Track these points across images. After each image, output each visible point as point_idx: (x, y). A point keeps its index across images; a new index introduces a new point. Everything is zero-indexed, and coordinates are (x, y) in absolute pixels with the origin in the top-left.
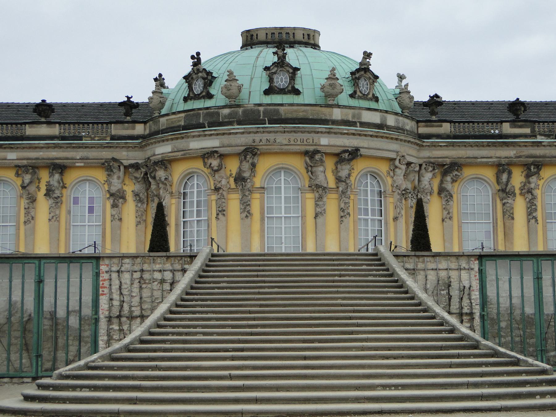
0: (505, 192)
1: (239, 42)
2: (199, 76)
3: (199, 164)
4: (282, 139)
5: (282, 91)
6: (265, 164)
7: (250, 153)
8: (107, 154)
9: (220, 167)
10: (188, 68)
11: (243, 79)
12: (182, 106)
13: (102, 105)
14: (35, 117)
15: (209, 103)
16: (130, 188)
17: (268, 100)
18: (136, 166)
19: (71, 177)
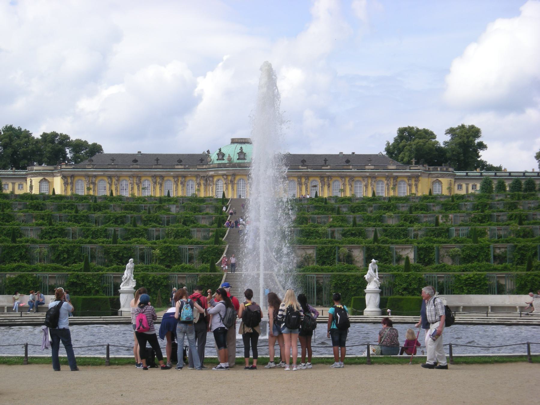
0: (300, 184)
1: (230, 141)
2: (221, 155)
3: (221, 177)
4: (241, 172)
5: (241, 159)
6: (237, 178)
7: (234, 175)
8: (196, 173)
9: (227, 178)
10: (218, 151)
11: (232, 156)
12: (216, 162)
13: (188, 155)
14: (177, 163)
15: (223, 162)
16: (202, 182)
17: (238, 161)
18: (204, 177)
19: (188, 179)
